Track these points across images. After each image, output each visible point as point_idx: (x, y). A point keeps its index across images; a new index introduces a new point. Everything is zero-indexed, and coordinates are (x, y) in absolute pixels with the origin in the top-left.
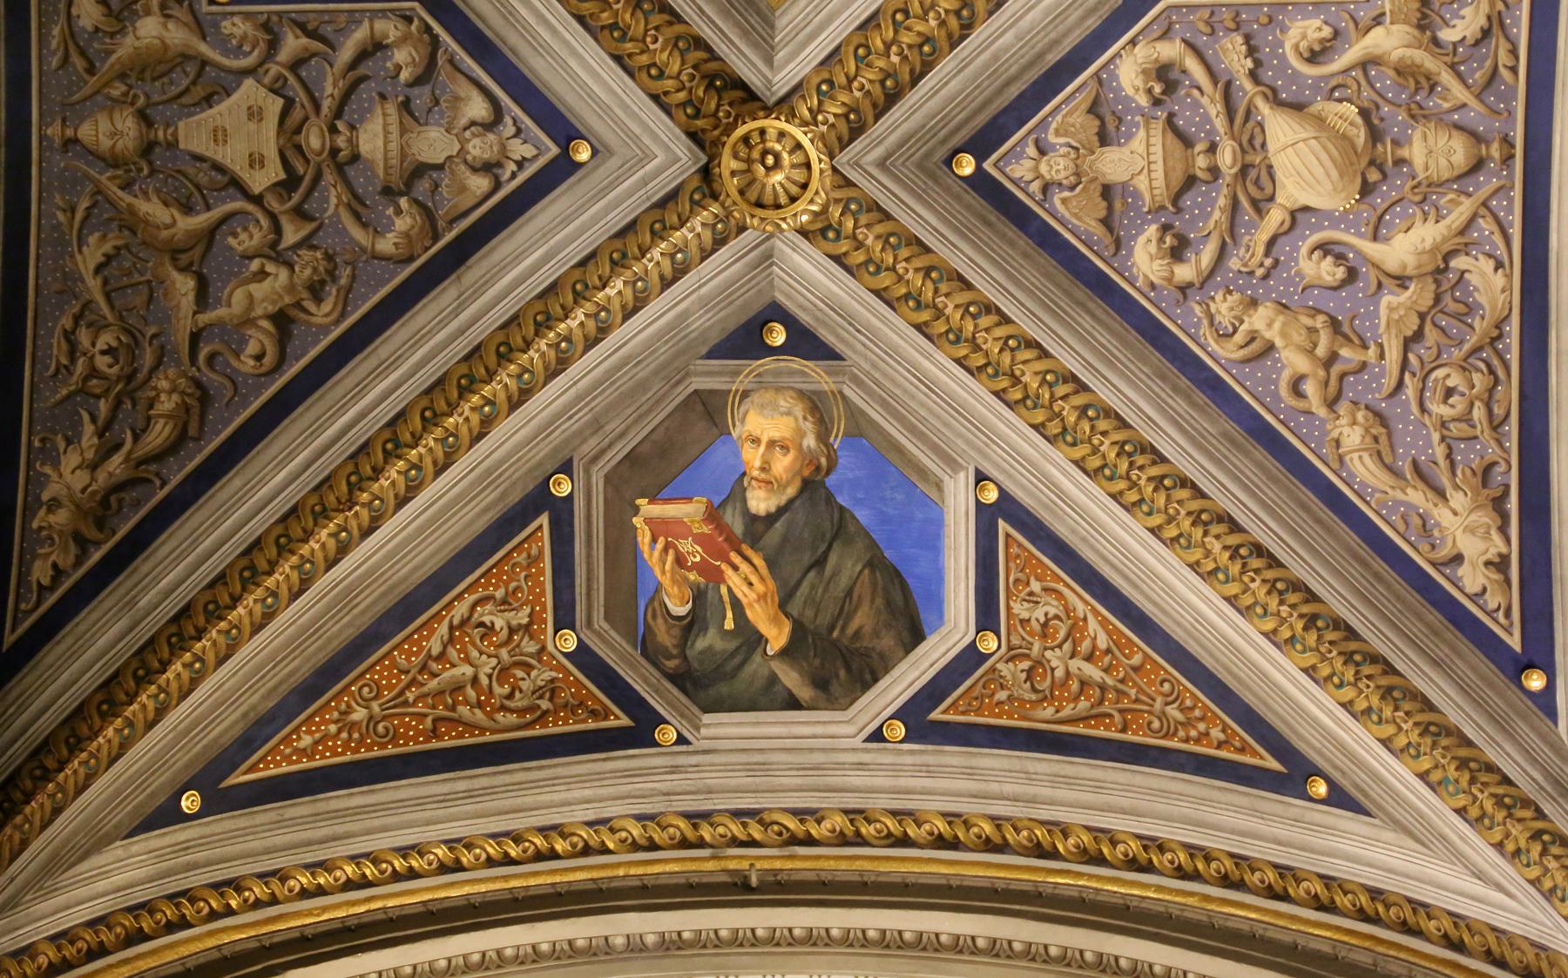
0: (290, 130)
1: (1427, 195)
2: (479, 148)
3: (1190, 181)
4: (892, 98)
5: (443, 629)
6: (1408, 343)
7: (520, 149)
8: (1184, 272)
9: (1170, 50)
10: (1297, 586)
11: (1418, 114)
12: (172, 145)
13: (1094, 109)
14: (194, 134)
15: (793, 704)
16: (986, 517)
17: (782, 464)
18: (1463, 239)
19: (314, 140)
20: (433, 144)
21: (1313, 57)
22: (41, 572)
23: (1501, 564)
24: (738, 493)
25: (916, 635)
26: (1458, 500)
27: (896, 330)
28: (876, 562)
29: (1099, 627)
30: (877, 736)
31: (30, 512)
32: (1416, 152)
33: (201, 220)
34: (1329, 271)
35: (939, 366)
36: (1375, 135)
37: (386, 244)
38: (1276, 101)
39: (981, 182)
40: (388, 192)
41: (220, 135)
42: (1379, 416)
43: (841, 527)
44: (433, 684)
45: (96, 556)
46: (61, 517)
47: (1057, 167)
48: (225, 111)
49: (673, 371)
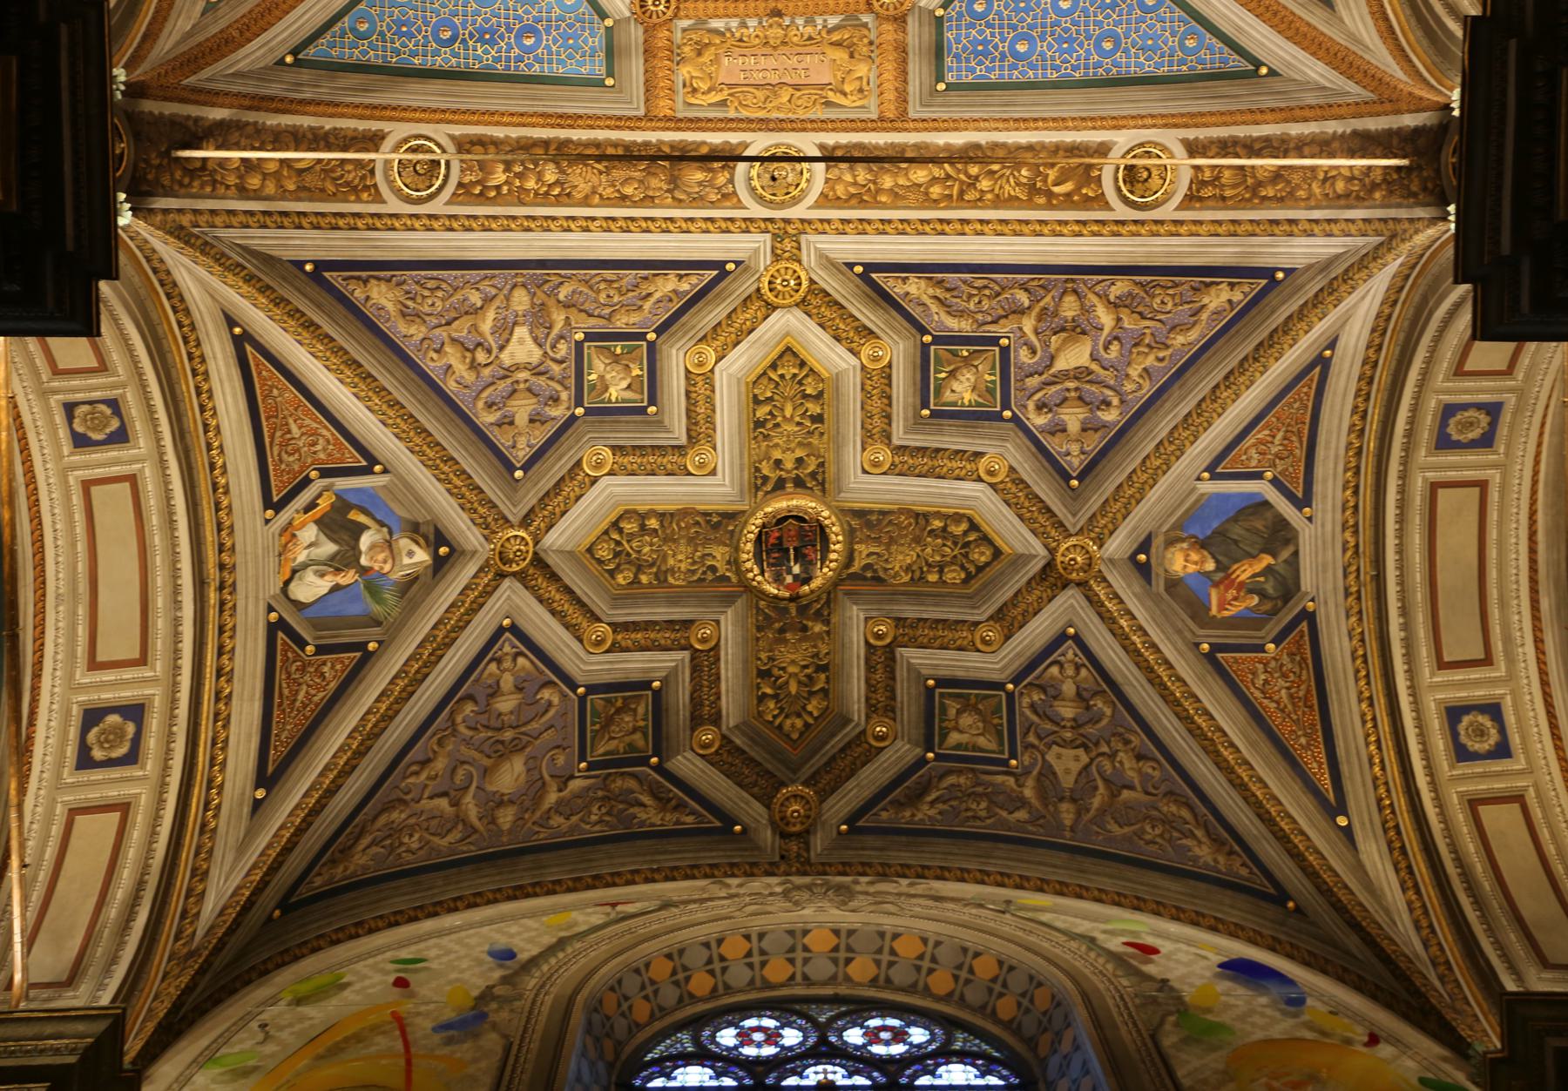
0: (1064, 744)
1: (1086, 310)
2: (1070, 671)
3: (1080, 398)
4: (1049, 510)
5: (1266, 702)
6: (1143, 317)
7: (1070, 655)
8: (1115, 401)
9: (1031, 405)
10: (1241, 363)
11: (1055, 314)
12: (1072, 790)
13: (1053, 434)
14: (1068, 782)
15: (1296, 554)
16: (1215, 477)
17: (1194, 556)
18: (1103, 297)
19: (1068, 735)
20: (1069, 688)
21: (1034, 352)
22: (1244, 872)
23: (1232, 285)
24: (1207, 574)
25: (1266, 504)
26: (1206, 300)
27: (1139, 512)
28: (1235, 519)
29: (1261, 433)
30: (1310, 519)
31: (1219, 872)
32: (1070, 314)
33: (1100, 783)
34: (1115, 347)
35: (1153, 495)
36: (1063, 329)
37: (1108, 711)
38: (1050, 366)
39: (1080, 478)
40: (1088, 708)
41: (1067, 771)
42: (1173, 328)
43: (1220, 533)
44: (1290, 707)
45: (1237, 848)
46: (1221, 859)
47: (1075, 448)
48: (1058, 768)
49: (1157, 599)
